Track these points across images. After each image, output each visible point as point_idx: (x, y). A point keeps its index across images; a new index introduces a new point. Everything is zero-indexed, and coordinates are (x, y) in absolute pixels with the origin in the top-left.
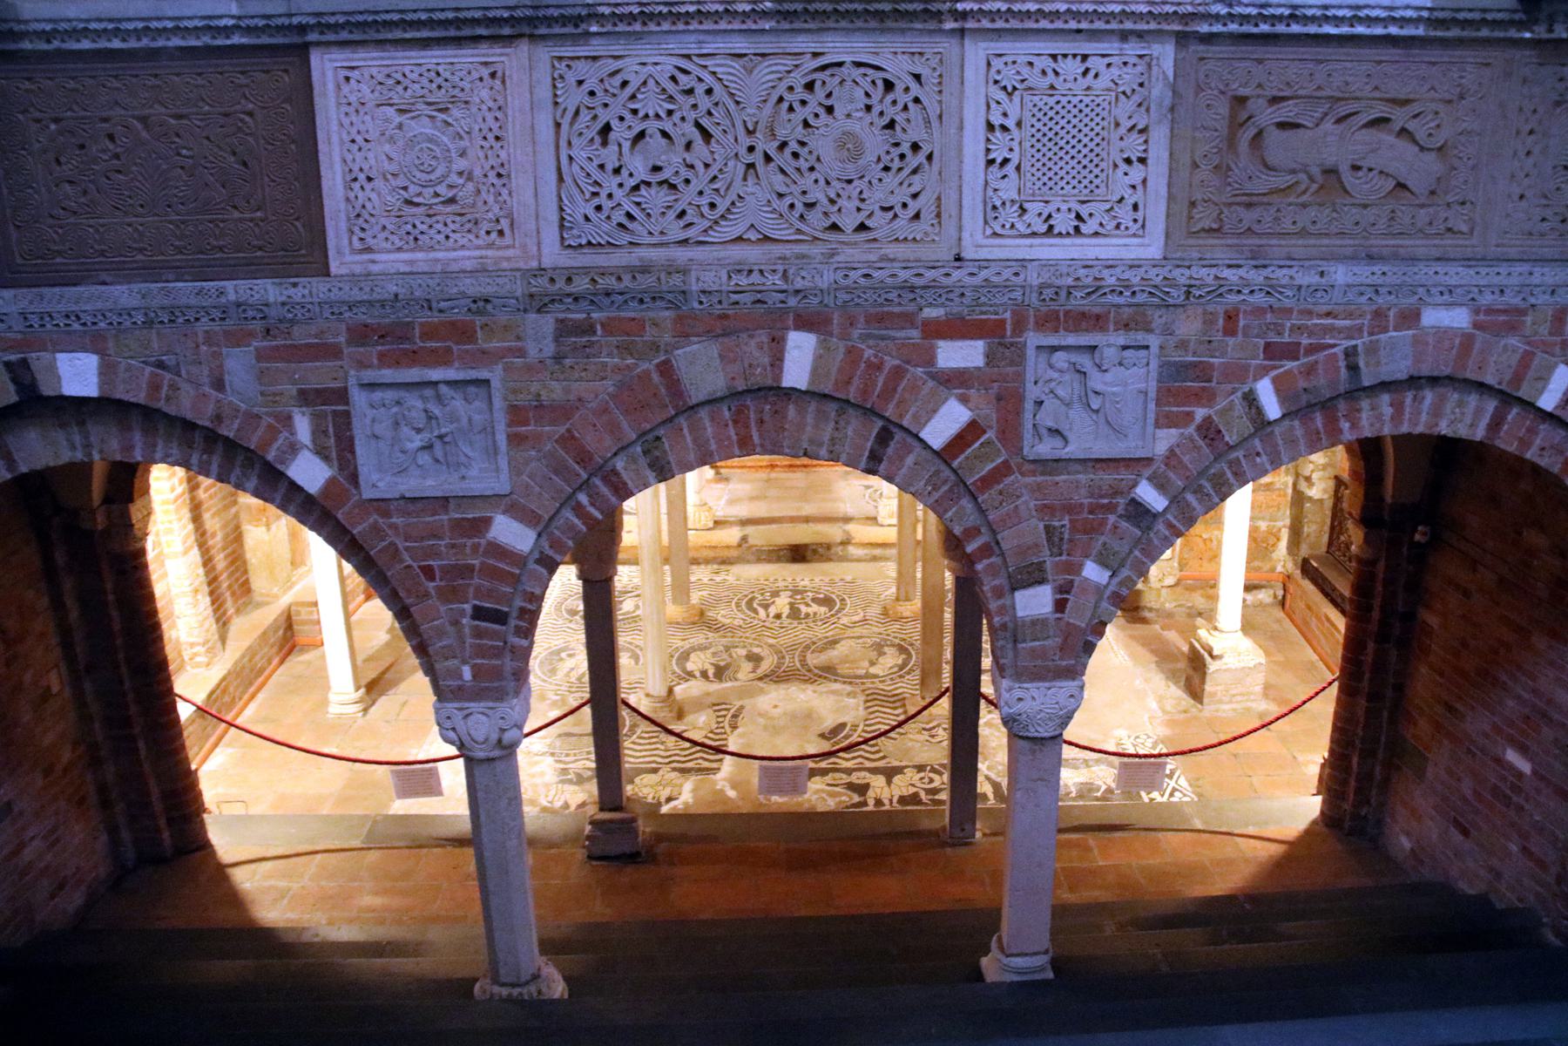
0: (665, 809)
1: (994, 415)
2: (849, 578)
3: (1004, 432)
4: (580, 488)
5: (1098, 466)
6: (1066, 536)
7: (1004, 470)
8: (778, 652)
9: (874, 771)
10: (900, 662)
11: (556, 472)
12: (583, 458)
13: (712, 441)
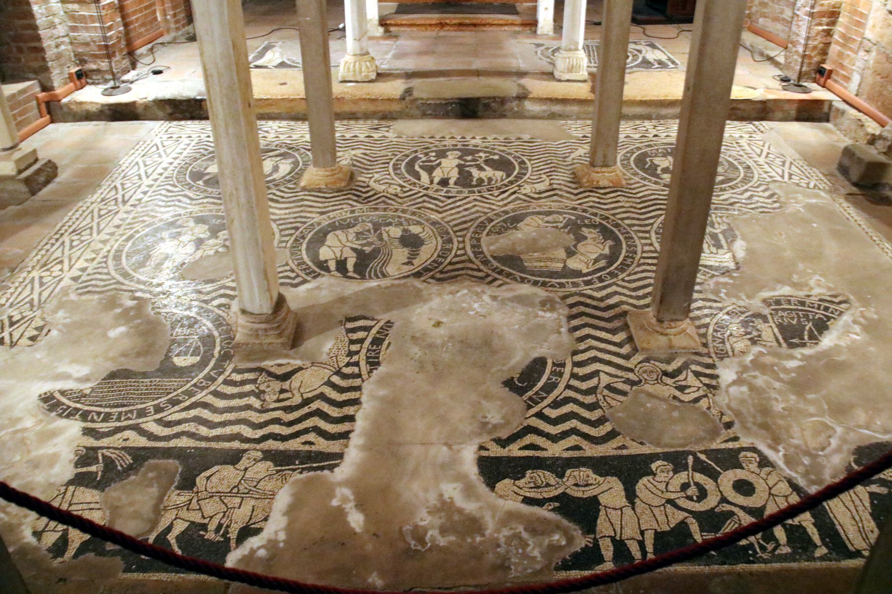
2: (526, 137)
8: (444, 233)
9: (602, 466)
10: (607, 251)
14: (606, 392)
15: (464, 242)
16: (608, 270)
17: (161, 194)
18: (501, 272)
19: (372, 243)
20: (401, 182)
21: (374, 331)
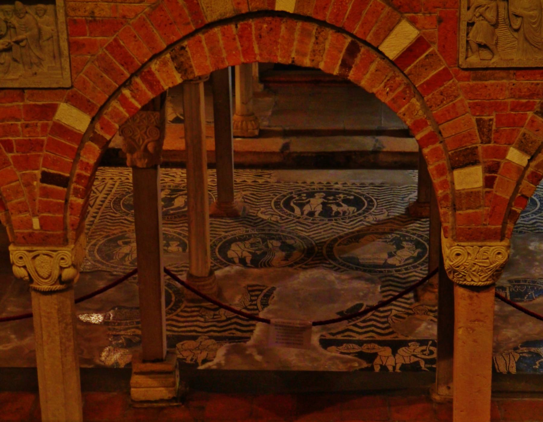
0: (201, 367)
1: (437, 34)
3: (444, 46)
4: (124, 85)
5: (519, 73)
6: (494, 128)
7: (444, 76)
10: (416, 254)
11: (106, 71)
12: (126, 61)
13: (224, 51)
14: (394, 317)
15: (322, 249)
16: (413, 265)
17: (107, 218)
18: (344, 265)
19: (261, 249)
20: (280, 213)
21: (265, 291)
